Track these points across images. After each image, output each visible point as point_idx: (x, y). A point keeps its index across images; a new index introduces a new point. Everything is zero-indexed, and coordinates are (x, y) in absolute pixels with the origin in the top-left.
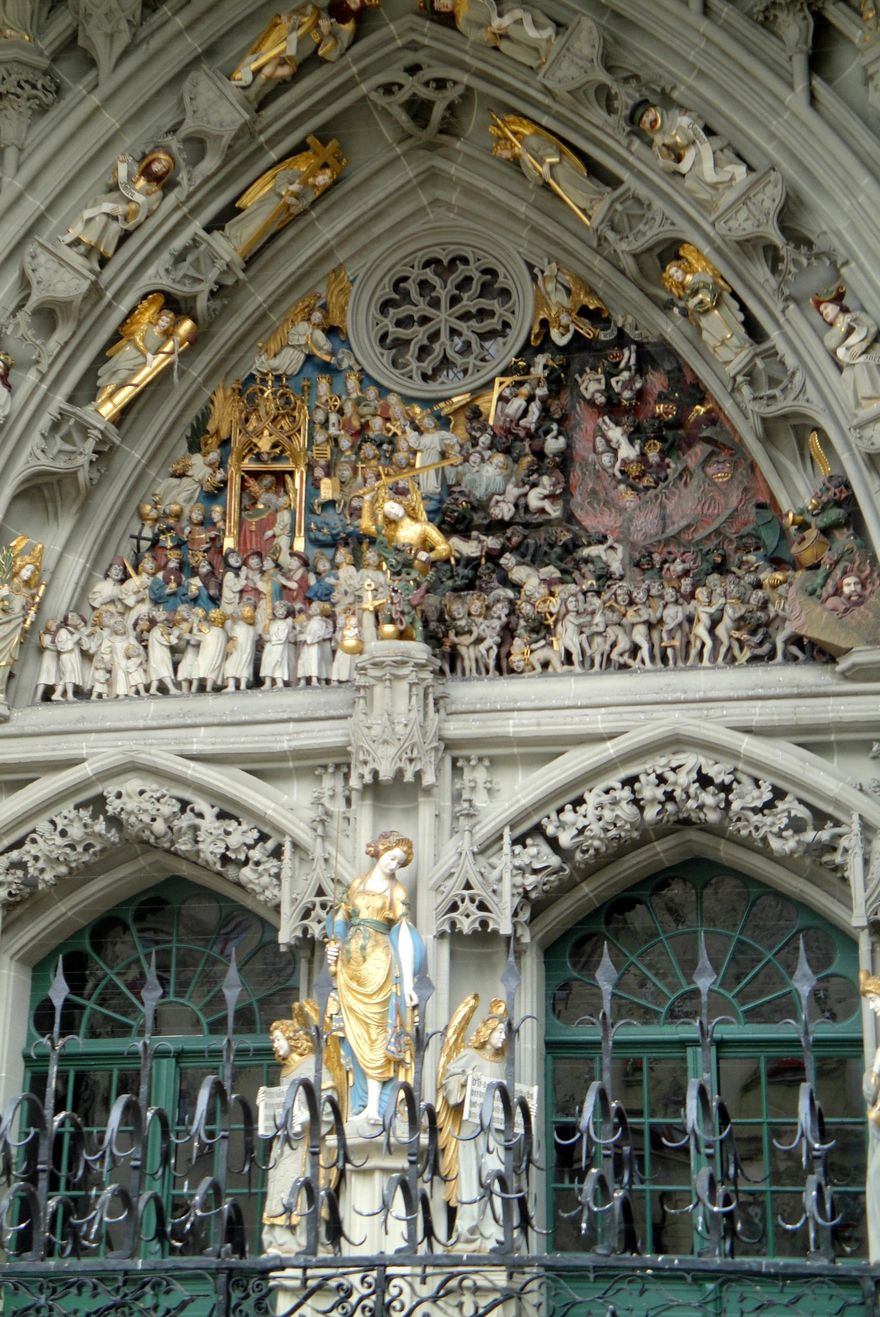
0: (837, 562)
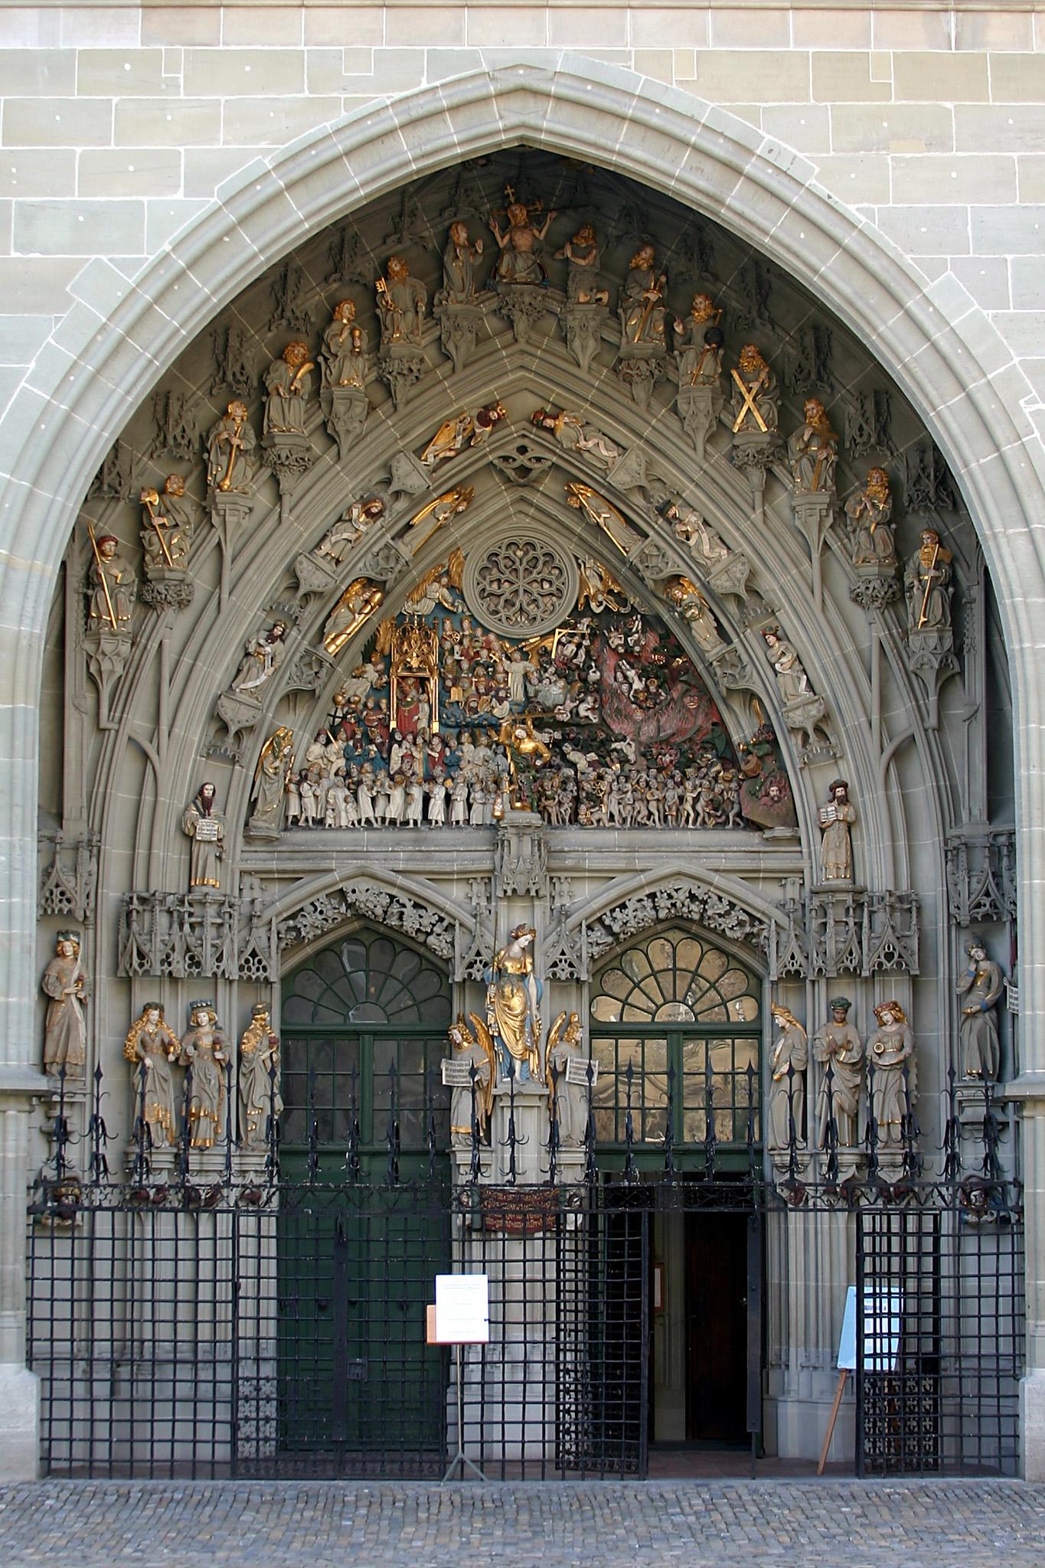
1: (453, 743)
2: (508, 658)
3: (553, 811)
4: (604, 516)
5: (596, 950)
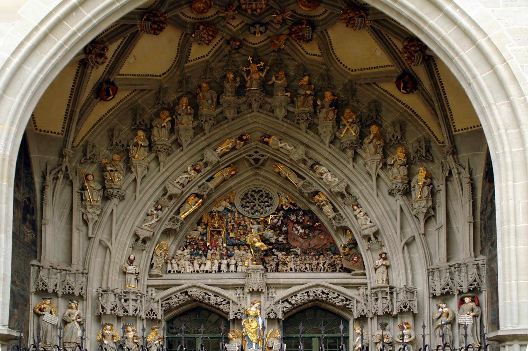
0: (352, 255)
1: (231, 250)
2: (252, 224)
3: (269, 268)
4: (288, 174)
5: (285, 309)
